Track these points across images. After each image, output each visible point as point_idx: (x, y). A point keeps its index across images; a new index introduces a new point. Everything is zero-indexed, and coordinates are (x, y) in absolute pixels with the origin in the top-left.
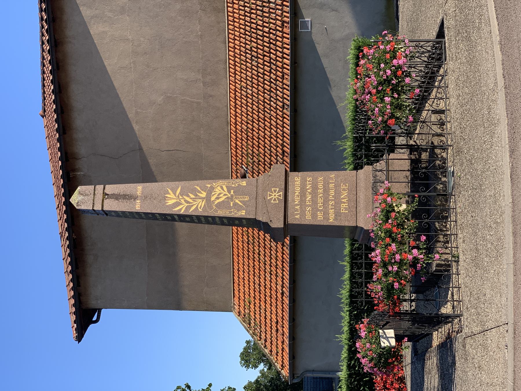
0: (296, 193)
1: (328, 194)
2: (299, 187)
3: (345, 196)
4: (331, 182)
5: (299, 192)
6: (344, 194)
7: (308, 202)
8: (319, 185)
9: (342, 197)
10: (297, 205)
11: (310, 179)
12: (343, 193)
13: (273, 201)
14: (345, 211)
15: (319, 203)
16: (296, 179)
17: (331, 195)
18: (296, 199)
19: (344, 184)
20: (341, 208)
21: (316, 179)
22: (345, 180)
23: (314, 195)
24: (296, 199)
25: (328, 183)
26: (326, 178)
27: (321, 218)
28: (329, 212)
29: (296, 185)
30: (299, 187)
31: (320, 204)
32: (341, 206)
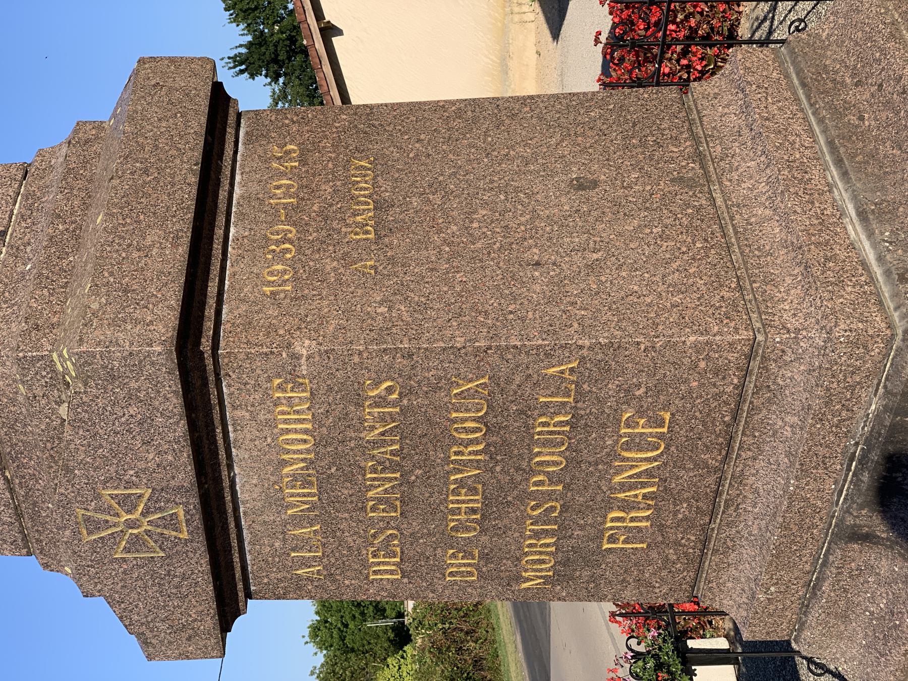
0: (284, 463)
1: (518, 469)
2: (306, 431)
3: (639, 475)
4: (547, 405)
5: (312, 462)
6: (632, 467)
7: (374, 509)
8: (454, 421)
9: (617, 479)
10: (298, 521)
11: (389, 390)
12: (624, 459)
13: (127, 550)
14: (624, 542)
15: (453, 512)
16: (280, 387)
17: (539, 473)
18: (292, 495)
19: (640, 413)
20: (602, 532)
21: (436, 389)
22: (657, 390)
23: (419, 472)
24: (292, 495)
25: (521, 412)
26: (509, 381)
27: (470, 574)
28: (520, 548)
29: (286, 421)
30: (306, 431)
31: (463, 517)
32: (604, 522)
